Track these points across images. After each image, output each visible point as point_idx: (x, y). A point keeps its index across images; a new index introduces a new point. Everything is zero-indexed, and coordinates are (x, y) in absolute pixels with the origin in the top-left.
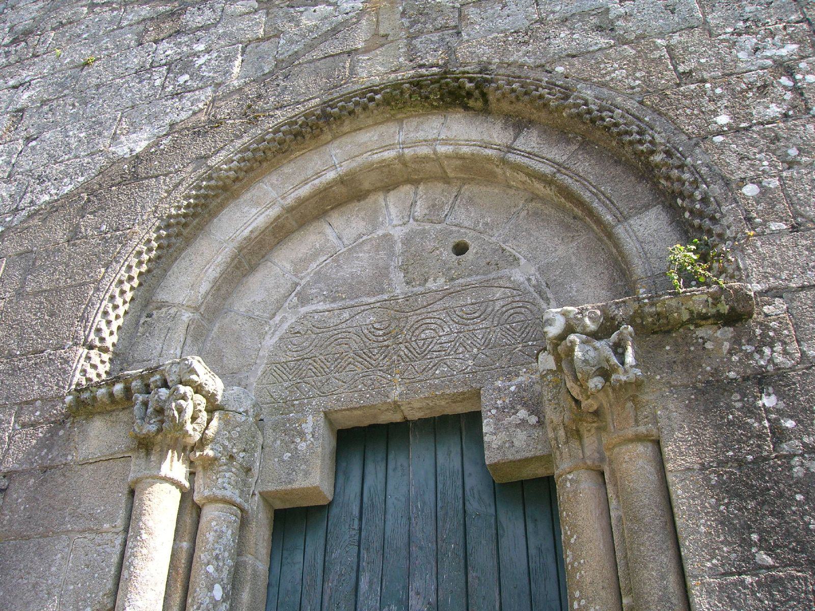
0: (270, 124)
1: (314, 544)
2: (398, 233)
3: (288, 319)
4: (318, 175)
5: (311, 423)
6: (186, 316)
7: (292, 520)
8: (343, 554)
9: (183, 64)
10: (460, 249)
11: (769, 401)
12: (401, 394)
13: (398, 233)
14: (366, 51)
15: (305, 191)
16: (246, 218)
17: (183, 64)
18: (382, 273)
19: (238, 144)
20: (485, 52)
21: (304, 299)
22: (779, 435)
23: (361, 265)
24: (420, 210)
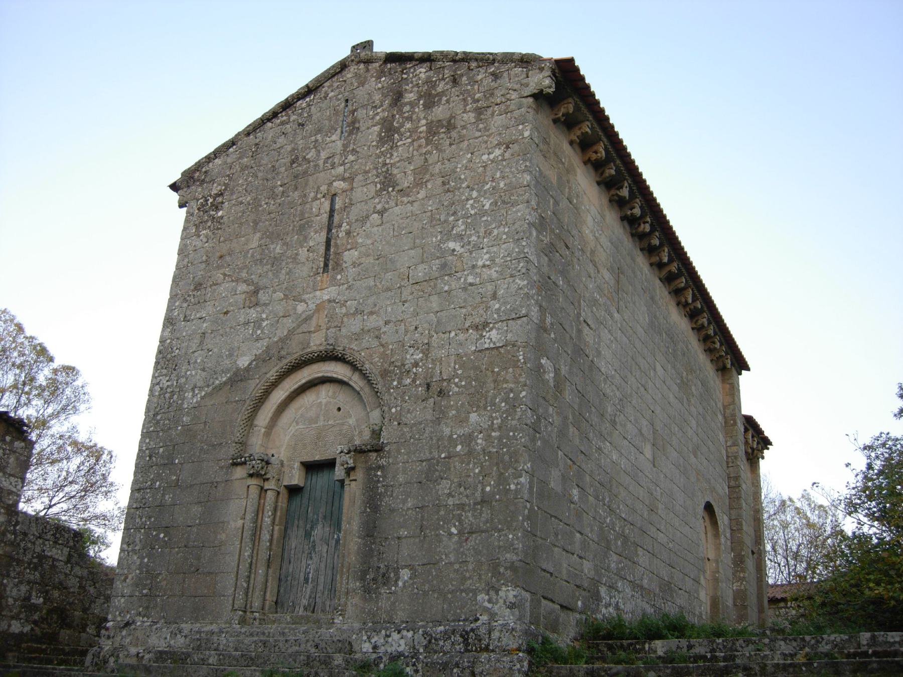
0: (285, 361)
1: (298, 499)
3: (292, 429)
4: (300, 380)
5: (297, 465)
6: (263, 430)
7: (294, 491)
8: (305, 501)
9: (258, 323)
10: (339, 409)
11: (379, 473)
12: (318, 457)
13: (324, 401)
15: (296, 386)
16: (279, 395)
17: (258, 323)
18: (318, 417)
19: (275, 369)
21: (297, 423)
22: (378, 481)
23: (312, 414)
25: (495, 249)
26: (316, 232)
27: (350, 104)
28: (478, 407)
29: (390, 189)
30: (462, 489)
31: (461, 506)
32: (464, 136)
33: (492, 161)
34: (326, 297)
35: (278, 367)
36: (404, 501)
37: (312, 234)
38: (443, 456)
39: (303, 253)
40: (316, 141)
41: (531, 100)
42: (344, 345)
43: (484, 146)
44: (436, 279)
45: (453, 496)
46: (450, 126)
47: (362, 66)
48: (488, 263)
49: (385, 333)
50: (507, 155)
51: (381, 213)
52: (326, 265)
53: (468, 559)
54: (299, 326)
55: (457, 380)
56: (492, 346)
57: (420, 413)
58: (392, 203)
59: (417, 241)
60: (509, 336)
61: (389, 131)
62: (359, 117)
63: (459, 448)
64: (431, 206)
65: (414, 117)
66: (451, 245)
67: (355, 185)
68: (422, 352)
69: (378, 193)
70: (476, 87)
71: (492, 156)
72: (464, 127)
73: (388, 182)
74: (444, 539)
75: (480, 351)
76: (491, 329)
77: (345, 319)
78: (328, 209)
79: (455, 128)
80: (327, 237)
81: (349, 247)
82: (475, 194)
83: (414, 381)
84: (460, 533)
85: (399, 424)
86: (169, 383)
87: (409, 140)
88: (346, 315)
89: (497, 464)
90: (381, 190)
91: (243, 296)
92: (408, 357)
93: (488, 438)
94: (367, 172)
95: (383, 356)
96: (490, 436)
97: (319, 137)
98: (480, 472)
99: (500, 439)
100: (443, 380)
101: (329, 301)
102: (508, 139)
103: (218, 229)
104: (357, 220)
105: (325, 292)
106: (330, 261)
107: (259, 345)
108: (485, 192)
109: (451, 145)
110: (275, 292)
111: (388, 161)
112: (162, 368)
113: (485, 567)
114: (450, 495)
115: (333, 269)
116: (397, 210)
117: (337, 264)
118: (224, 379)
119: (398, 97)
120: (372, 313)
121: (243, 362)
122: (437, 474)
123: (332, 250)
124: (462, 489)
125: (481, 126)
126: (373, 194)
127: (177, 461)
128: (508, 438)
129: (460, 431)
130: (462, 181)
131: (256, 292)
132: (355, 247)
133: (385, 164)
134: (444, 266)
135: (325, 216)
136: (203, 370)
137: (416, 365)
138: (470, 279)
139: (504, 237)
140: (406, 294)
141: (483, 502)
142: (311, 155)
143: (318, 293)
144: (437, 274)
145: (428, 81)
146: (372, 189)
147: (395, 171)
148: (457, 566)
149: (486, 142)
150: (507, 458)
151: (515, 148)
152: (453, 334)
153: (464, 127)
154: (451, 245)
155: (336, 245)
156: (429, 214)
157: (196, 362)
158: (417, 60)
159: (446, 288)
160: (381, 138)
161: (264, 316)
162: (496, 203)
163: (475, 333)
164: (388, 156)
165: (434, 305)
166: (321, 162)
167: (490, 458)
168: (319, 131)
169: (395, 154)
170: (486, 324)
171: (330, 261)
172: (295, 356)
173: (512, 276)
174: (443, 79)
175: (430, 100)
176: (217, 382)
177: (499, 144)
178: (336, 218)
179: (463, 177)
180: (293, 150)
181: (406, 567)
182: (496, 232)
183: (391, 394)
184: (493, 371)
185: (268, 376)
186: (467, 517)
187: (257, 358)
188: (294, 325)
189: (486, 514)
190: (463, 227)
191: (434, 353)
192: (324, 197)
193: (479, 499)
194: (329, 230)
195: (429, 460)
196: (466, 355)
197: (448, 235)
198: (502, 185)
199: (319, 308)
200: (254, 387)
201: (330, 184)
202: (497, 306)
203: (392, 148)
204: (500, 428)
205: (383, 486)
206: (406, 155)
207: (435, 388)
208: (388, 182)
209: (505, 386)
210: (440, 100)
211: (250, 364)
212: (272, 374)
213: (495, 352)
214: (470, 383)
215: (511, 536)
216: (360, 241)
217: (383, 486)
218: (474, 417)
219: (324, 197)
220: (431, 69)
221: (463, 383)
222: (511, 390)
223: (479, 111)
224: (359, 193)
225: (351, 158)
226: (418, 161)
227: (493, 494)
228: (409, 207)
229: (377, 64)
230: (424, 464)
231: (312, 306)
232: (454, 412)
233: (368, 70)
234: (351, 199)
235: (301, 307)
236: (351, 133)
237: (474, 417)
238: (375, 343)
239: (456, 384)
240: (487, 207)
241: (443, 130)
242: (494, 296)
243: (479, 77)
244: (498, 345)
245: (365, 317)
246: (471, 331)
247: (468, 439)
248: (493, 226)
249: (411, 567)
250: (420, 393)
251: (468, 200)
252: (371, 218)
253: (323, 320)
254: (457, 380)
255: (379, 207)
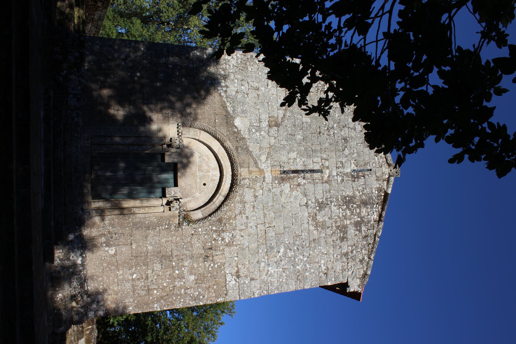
2: (210, 174)
9: (259, 129)
10: (205, 184)
14: (249, 170)
17: (259, 129)
18: (202, 171)
19: (231, 146)
20: (241, 192)
23: (205, 167)
24: (214, 178)
25: (276, 276)
26: (303, 162)
27: (368, 173)
28: (197, 280)
29: (318, 208)
30: (156, 277)
31: (147, 278)
32: (336, 247)
33: (320, 266)
34: (266, 176)
35: (232, 148)
36: (151, 244)
37: (303, 160)
38: (174, 263)
39: (293, 155)
40: (353, 154)
41: (345, 281)
42: (238, 190)
43: (329, 260)
44: (266, 244)
45: (152, 273)
46: (342, 239)
47: (387, 176)
48: (269, 273)
49: (242, 217)
50: (321, 274)
51: (307, 205)
52: (284, 172)
53: (120, 286)
54: (253, 158)
55: (212, 265)
56: (227, 282)
57: (197, 246)
58: (310, 210)
59: (287, 230)
60: (231, 291)
61: (348, 201)
62: (360, 180)
63: (177, 272)
64: (304, 235)
65: (352, 216)
66: (282, 250)
67: (325, 184)
68: (229, 242)
69: (317, 200)
70: (359, 250)
71: (322, 266)
72: (340, 247)
73: (321, 206)
74: (130, 271)
75: (225, 276)
76: (236, 281)
77: (253, 190)
78: (315, 168)
79: (341, 242)
80: (299, 171)
81: (292, 186)
82: (305, 259)
83: (215, 239)
84: (133, 280)
85: (192, 234)
86: (232, 66)
87: (341, 216)
88: (255, 190)
89: (168, 295)
90: (318, 202)
91: (276, 116)
92: (228, 234)
93: (181, 287)
94: (330, 192)
95: (230, 218)
96: (182, 289)
97: (355, 155)
98: (164, 286)
99: (181, 295)
100: (213, 257)
101: (264, 178)
102: (329, 273)
103: (318, 89)
104: (305, 189)
105: (270, 174)
106: (287, 175)
107: (247, 132)
108: (305, 265)
109: (333, 241)
110: (275, 138)
111: (333, 204)
112: (242, 59)
113: (115, 297)
114: (153, 270)
115: (282, 178)
116: (306, 214)
117: (283, 179)
118: (229, 109)
119: (365, 203)
120: (254, 207)
121: (237, 122)
122: (164, 262)
123: (292, 175)
124: (156, 277)
125: (339, 257)
126: (318, 198)
127: (183, 80)
128: (180, 299)
129: (185, 272)
130: (313, 251)
131: (277, 125)
132: (292, 190)
133: (331, 202)
134: (272, 248)
135: (310, 167)
136: (237, 92)
137: (223, 239)
138: (263, 264)
139: (281, 280)
140: (261, 227)
141: (149, 289)
142: (347, 152)
143: (269, 169)
144: (268, 244)
145: (369, 222)
146: (319, 197)
147: (326, 209)
148: (116, 280)
149: (330, 261)
150: (171, 300)
151: (324, 278)
152: (236, 258)
153: (340, 247)
154: (282, 250)
155: (294, 177)
156: (300, 234)
157: (242, 85)
158: (381, 212)
159: (260, 251)
160: (345, 197)
161: (262, 133)
162: (299, 272)
163: (235, 271)
164: (336, 204)
165: (253, 245)
166: (341, 160)
167: (171, 291)
168: (359, 155)
169: (335, 208)
170: (238, 277)
171: (287, 175)
172: (237, 159)
173: (261, 287)
174: (368, 229)
175: (358, 225)
176: (228, 104)
177: (328, 269)
178: (308, 175)
179: (316, 251)
180: (352, 138)
181: (116, 251)
182: (284, 274)
183: (208, 227)
184: (214, 285)
185: (228, 141)
186: (141, 282)
187: (239, 132)
188: (254, 155)
189: (143, 293)
190: (290, 255)
191: (227, 249)
192: (322, 165)
193: (150, 288)
194: (303, 171)
195: (172, 256)
196: (224, 268)
197: (288, 248)
198: (307, 274)
199: (261, 171)
200: (222, 131)
201: (328, 168)
202: (247, 282)
203: (339, 205)
204: (186, 293)
205: (160, 230)
206: (333, 215)
207: (210, 252)
208: (321, 206)
209: (206, 292)
210: (357, 230)
211: (236, 127)
212: (228, 144)
213: (224, 284)
214: (210, 273)
215: (131, 308)
216: (294, 193)
217: (160, 230)
218: (192, 278)
219: (322, 165)
220: (374, 221)
221: (210, 269)
222: (204, 297)
223: (346, 255)
224: (320, 187)
225: (340, 179)
226: (329, 223)
227: (152, 295)
228: (306, 221)
229: (385, 187)
230: (170, 253)
231: (263, 166)
232: (196, 266)
233: (384, 181)
234: (317, 183)
235: (263, 158)
236: (353, 176)
237: (192, 278)
238: (237, 212)
239: (210, 265)
240: (298, 267)
241: (342, 235)
242: (252, 279)
243: (363, 251)
244: (227, 286)
245: (252, 203)
246: (236, 269)
247: (181, 277)
248: (287, 273)
249: (115, 254)
250: (207, 244)
251: (303, 255)
252: (305, 198)
253: (253, 175)
254: (212, 265)
255: (310, 202)
